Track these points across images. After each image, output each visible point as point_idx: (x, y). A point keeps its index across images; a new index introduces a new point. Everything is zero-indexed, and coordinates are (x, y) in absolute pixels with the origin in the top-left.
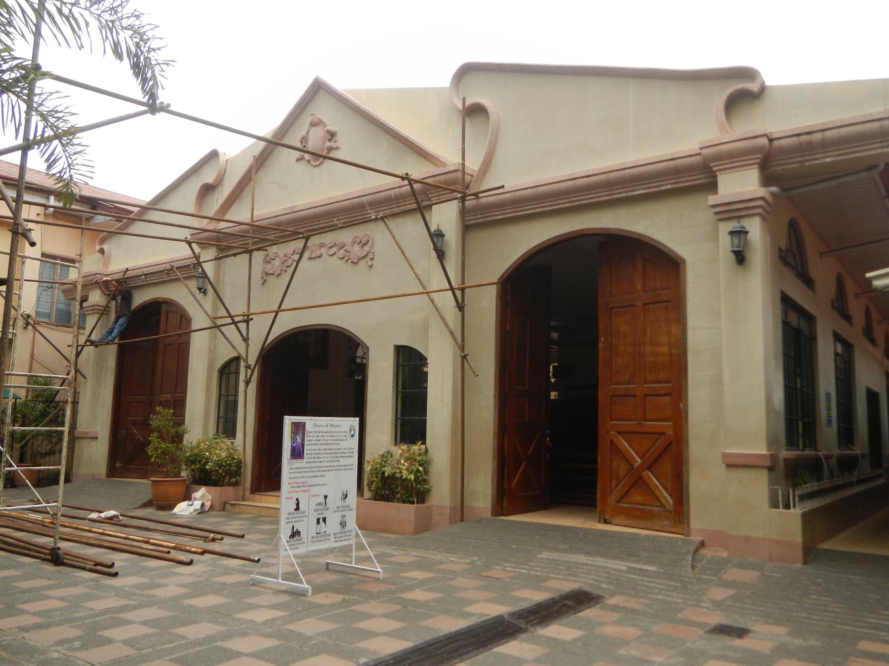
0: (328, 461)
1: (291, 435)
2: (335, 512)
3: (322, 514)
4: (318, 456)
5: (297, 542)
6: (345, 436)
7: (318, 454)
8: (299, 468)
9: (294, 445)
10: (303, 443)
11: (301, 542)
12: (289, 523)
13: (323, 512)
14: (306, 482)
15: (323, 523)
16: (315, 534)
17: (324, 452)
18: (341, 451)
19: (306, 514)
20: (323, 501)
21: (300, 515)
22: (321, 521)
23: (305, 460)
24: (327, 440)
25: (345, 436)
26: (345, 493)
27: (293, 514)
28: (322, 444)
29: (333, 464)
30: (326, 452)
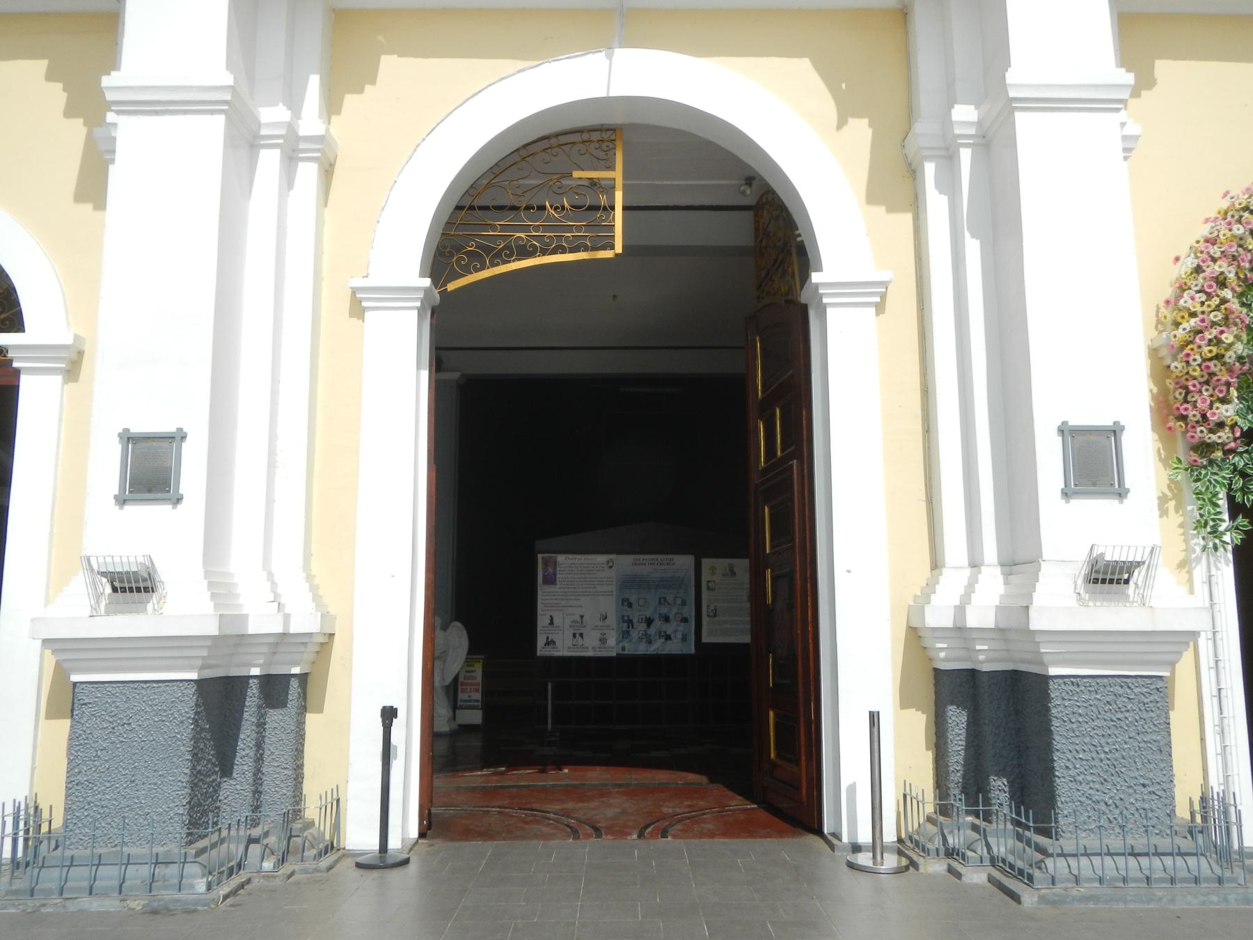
0: (583, 588)
2: (593, 629)
7: (571, 581)
15: (580, 638)
20: (579, 619)
22: (577, 635)
23: (558, 586)
27: (547, 627)
29: (588, 590)
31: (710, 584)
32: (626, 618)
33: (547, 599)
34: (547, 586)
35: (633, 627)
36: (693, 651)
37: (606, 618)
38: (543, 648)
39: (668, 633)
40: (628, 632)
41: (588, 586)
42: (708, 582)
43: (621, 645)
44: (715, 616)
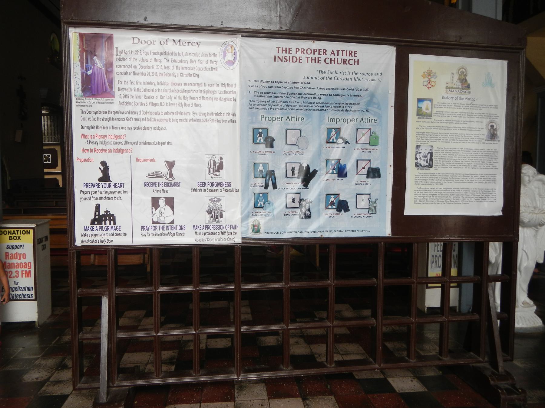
1: (81, 55)
3: (164, 191)
4: (148, 94)
5: (109, 232)
6: (212, 62)
7: (146, 90)
8: (104, 112)
9: (89, 73)
10: (110, 69)
11: (119, 232)
12: (88, 199)
13: (166, 189)
14: (123, 137)
15: (168, 208)
16: (150, 224)
17: (162, 87)
18: (202, 88)
19: (127, 187)
20: (165, 170)
21: (113, 189)
22: (162, 203)
23: (117, 100)
24: (167, 68)
25: (212, 62)
26: (218, 161)
28: (154, 74)
29: (184, 109)
30: (167, 87)
31: (424, 106)
32: (261, 167)
33: (93, 127)
34: (93, 100)
35: (275, 187)
36: (386, 231)
37: (221, 167)
38: (86, 229)
39: (342, 198)
40: (266, 195)
41: (183, 101)
42: (420, 100)
43: (251, 221)
44: (430, 166)
